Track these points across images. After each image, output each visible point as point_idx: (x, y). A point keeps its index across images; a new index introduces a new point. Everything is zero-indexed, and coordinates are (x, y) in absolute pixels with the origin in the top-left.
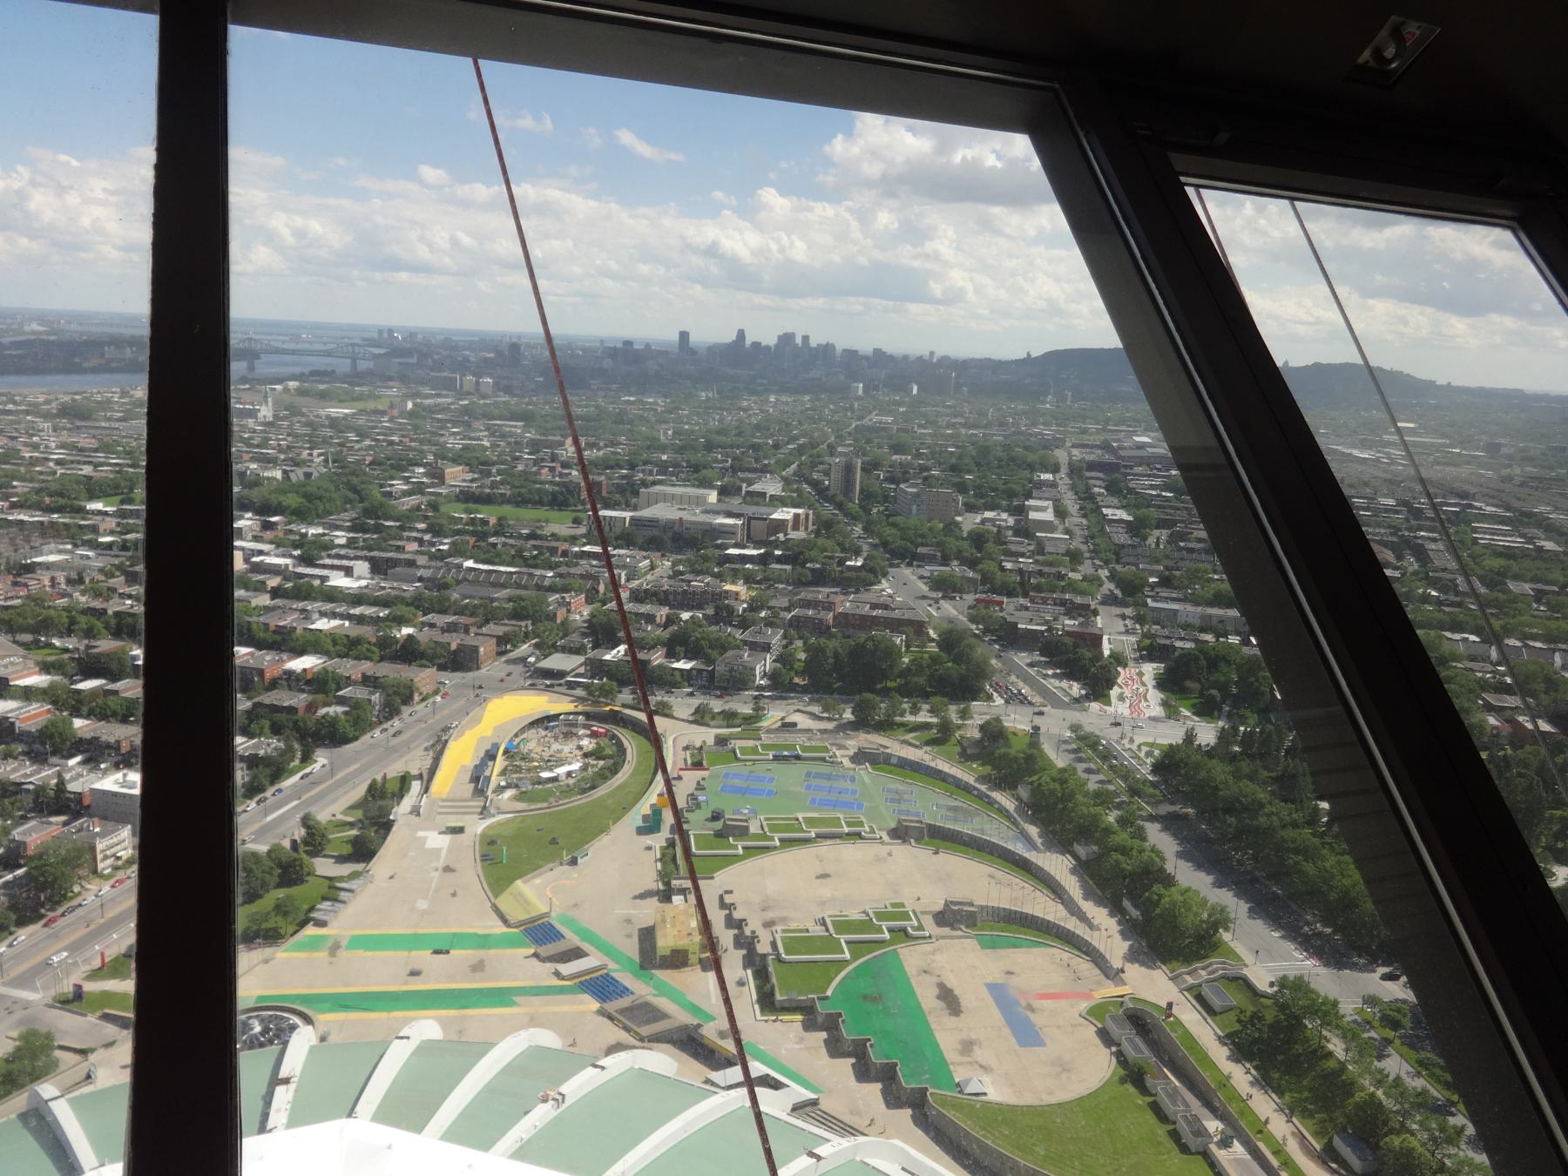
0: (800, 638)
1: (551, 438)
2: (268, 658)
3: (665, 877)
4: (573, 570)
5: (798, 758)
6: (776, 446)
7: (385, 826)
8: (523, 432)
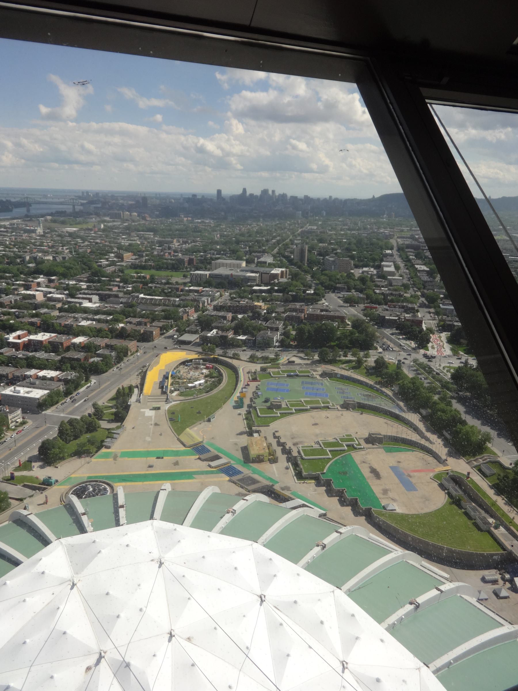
0: (291, 325)
1: (167, 239)
2: (64, 338)
3: (250, 426)
4: (187, 298)
5: (297, 375)
6: (267, 241)
7: (127, 408)
8: (154, 237)
